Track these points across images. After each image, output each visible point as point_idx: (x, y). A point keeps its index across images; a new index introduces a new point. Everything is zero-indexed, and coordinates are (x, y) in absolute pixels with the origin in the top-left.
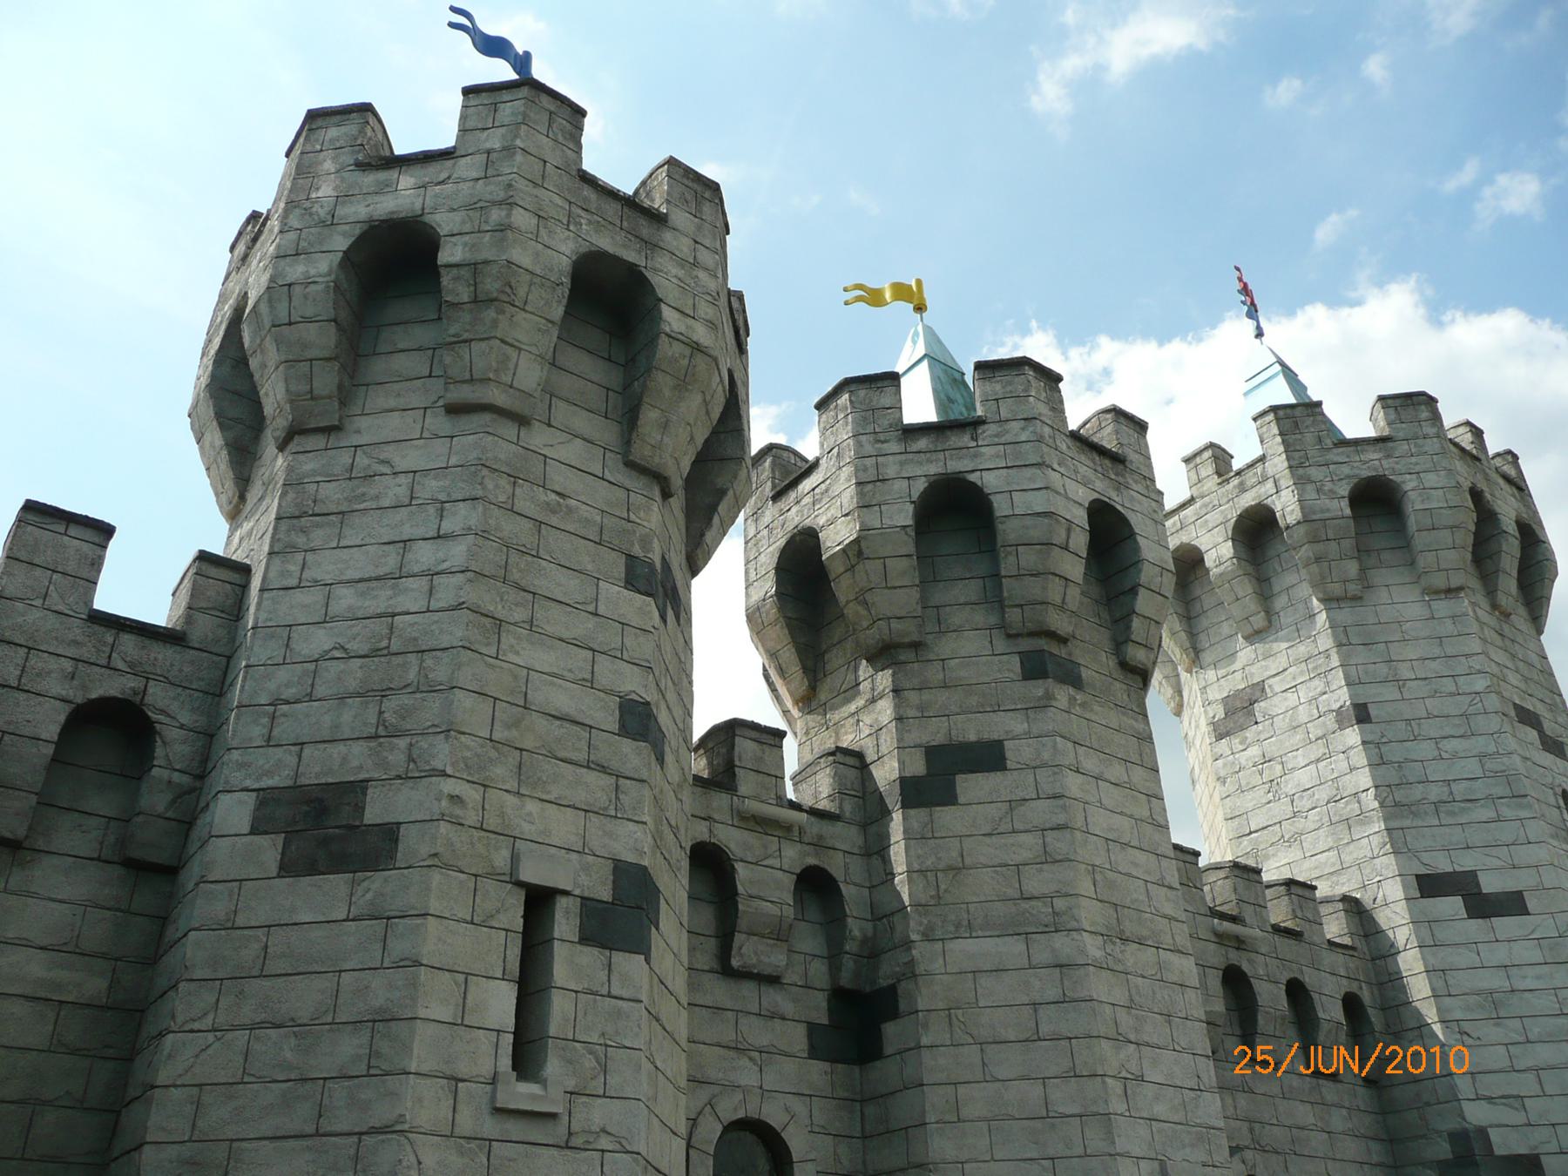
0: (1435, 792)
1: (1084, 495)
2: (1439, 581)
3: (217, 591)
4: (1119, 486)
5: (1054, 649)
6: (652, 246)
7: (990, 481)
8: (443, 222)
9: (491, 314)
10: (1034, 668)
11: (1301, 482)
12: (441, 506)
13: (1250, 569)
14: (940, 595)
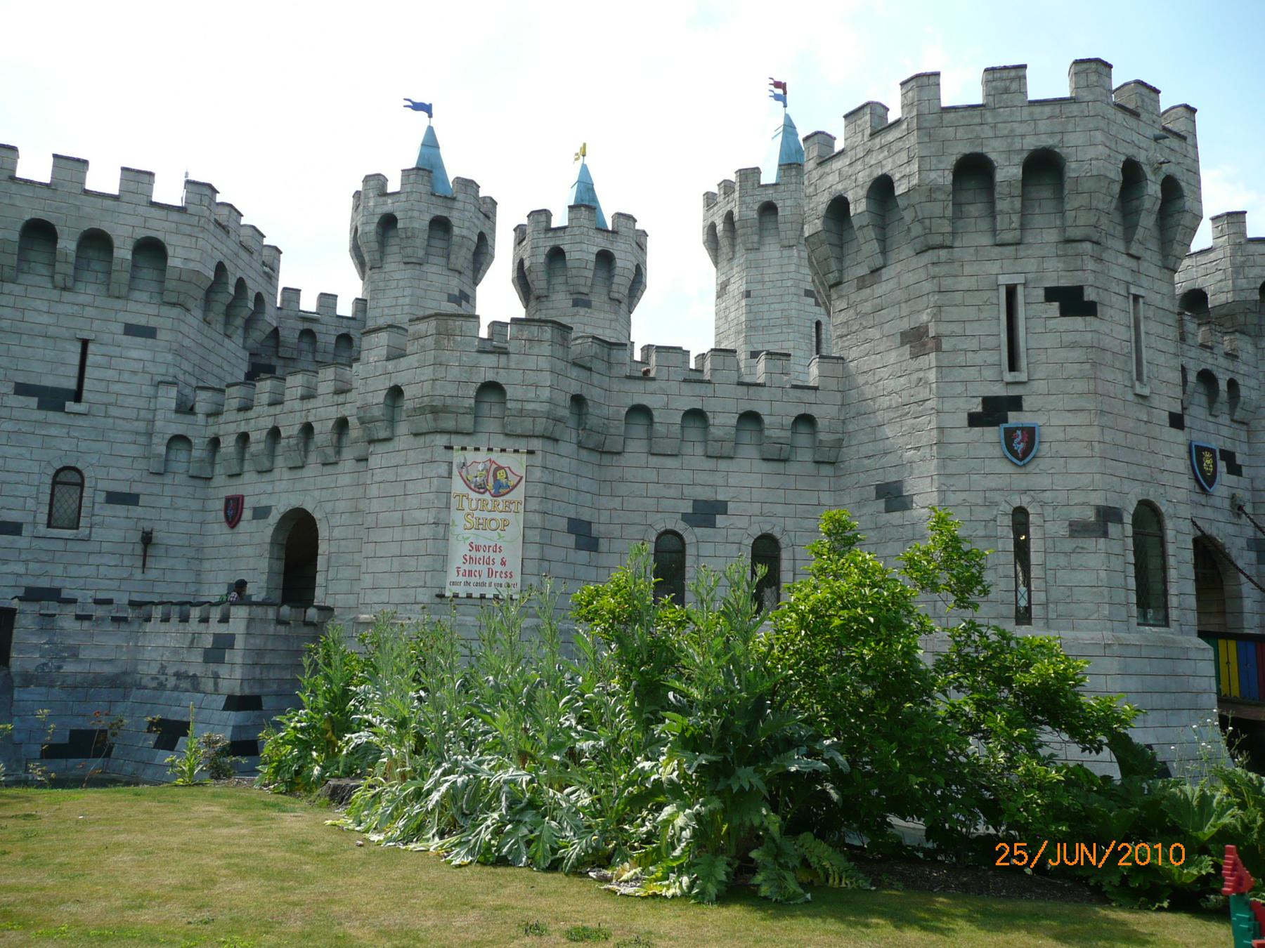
0: (764, 323)
1: (596, 250)
2: (786, 243)
3: (360, 306)
4: (612, 243)
5: (583, 297)
6: (451, 208)
7: (566, 248)
8: (398, 215)
9: (410, 241)
10: (576, 303)
11: (742, 203)
12: (404, 289)
13: (729, 234)
14: (554, 281)
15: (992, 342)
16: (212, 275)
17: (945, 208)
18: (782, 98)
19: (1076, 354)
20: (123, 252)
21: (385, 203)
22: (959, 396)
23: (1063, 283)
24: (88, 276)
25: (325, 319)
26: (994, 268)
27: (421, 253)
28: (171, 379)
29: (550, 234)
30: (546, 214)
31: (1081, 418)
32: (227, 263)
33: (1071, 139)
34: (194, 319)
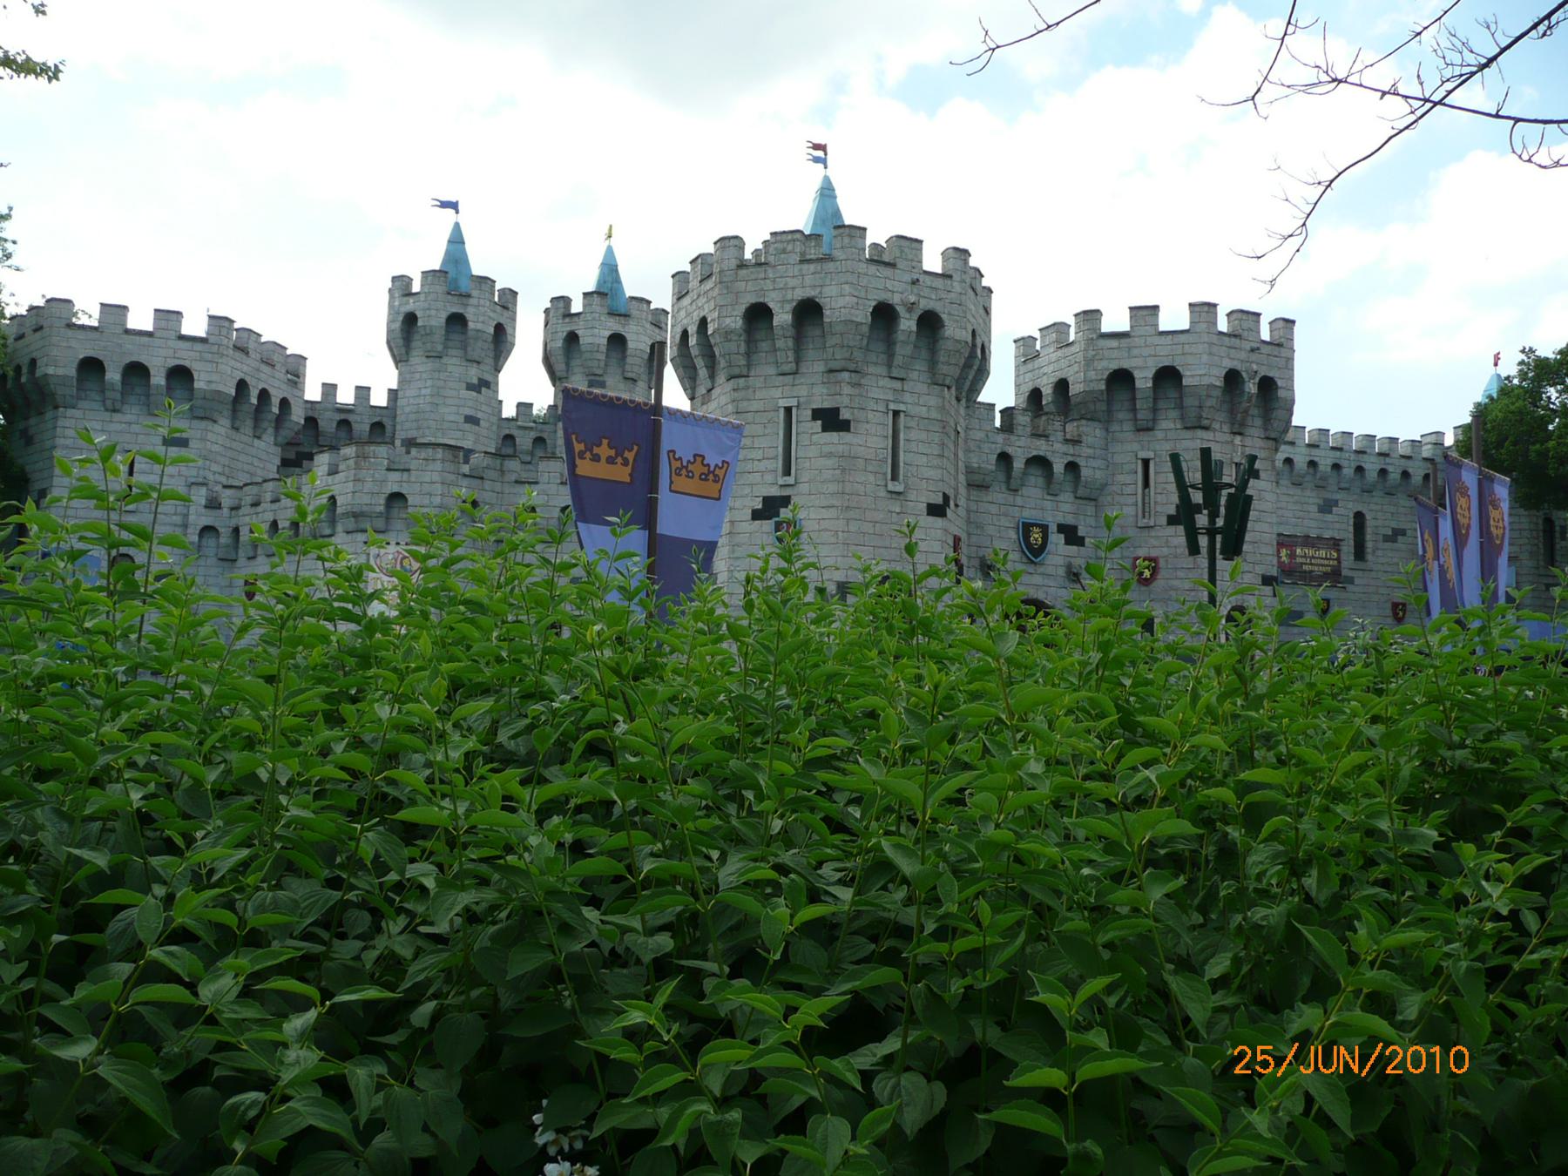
1: (607, 333)
6: (466, 305)
7: (580, 333)
8: (419, 314)
15: (771, 453)
16: (233, 392)
17: (738, 346)
18: (823, 161)
19: (830, 462)
20: (158, 379)
21: (408, 303)
22: (747, 496)
23: (826, 405)
24: (133, 399)
25: (359, 409)
26: (777, 393)
27: (440, 348)
28: (201, 480)
29: (567, 320)
30: (566, 301)
31: (832, 513)
32: (248, 379)
33: (828, 291)
34: (222, 428)
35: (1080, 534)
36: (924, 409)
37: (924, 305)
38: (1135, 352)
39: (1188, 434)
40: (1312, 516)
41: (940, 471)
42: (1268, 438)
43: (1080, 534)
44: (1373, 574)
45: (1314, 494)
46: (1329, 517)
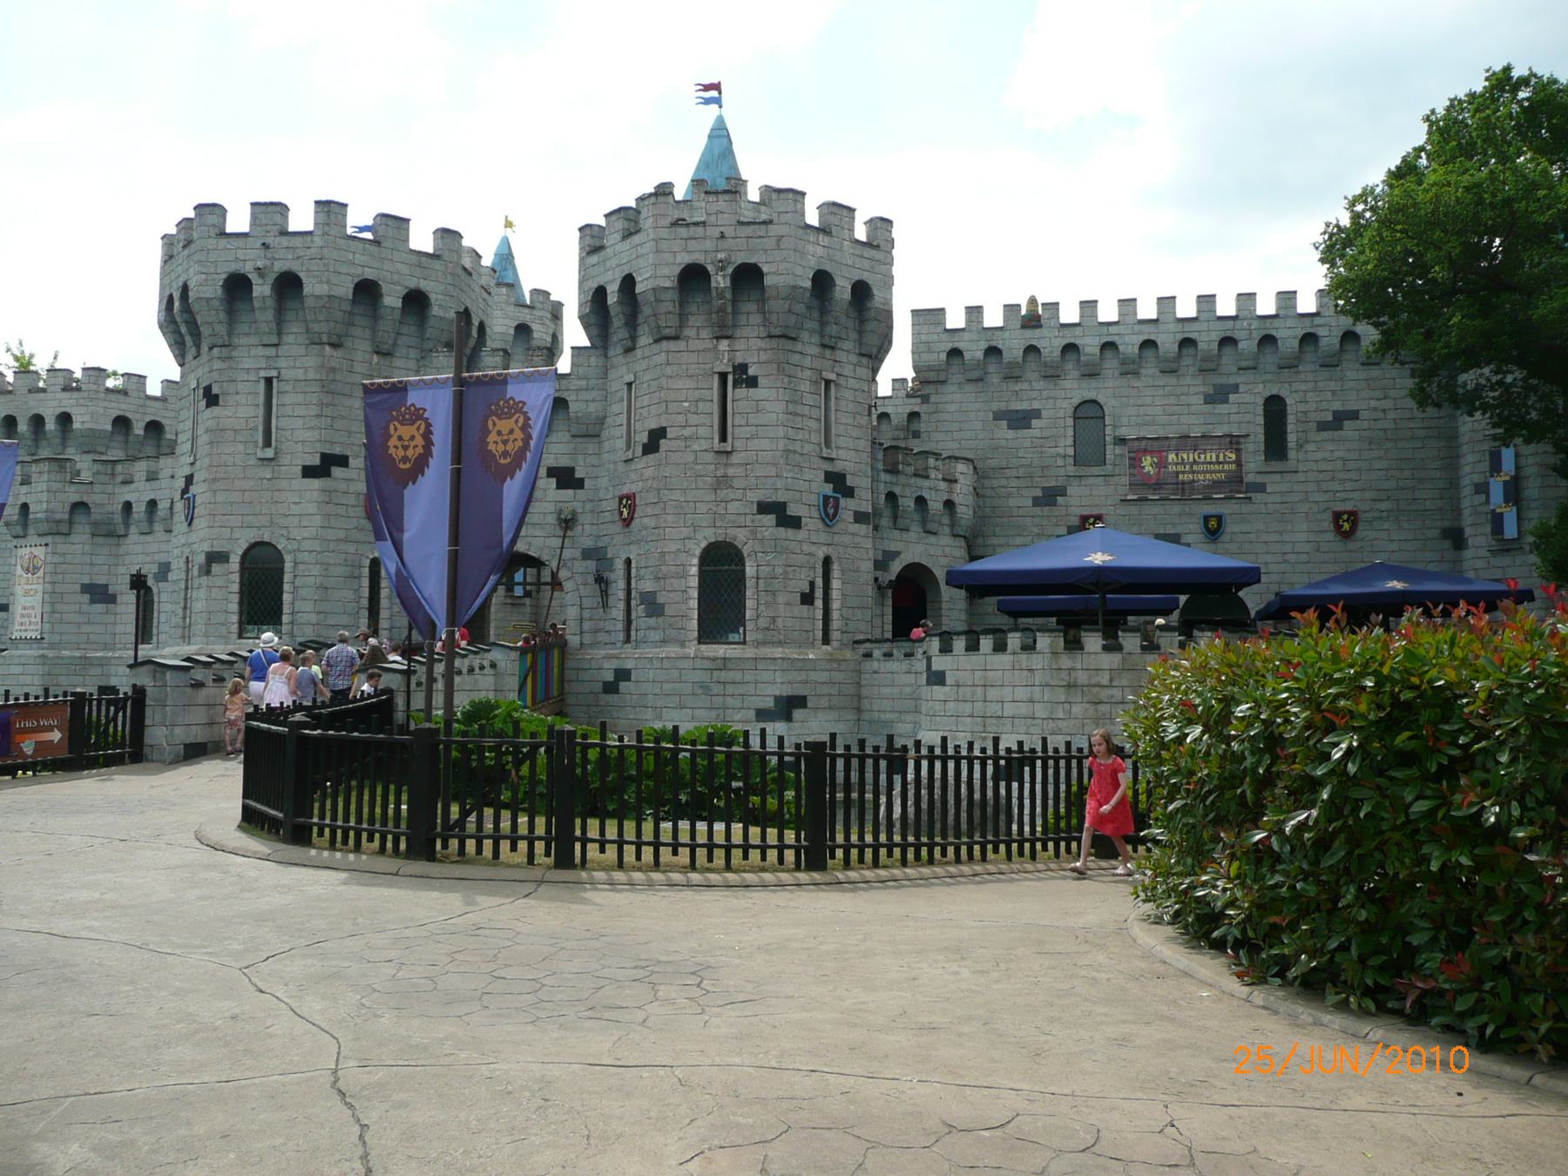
35: (554, 481)
36: (301, 371)
37: (280, 267)
38: (608, 264)
39: (657, 347)
40: (1193, 409)
41: (317, 432)
42: (770, 336)
43: (578, 475)
44: (1301, 477)
45: (1198, 381)
46: (1221, 408)
